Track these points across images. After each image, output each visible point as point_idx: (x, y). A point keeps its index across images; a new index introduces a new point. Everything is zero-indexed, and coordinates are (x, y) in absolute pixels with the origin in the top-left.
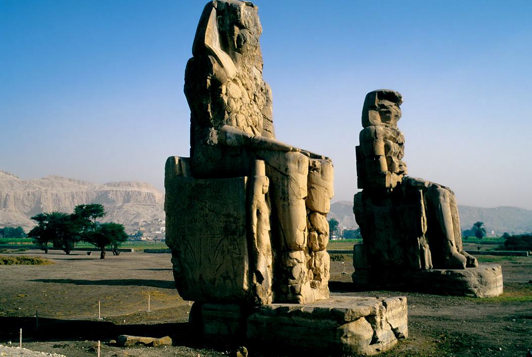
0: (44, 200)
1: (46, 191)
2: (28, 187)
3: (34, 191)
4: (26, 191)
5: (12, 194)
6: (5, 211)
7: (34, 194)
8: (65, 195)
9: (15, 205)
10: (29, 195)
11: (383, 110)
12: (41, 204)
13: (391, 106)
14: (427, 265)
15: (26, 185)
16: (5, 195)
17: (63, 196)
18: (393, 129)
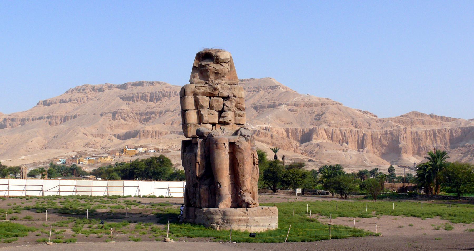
0: (402, 138)
1: (405, 130)
2: (386, 126)
3: (392, 130)
4: (383, 130)
5: (369, 134)
6: (362, 151)
7: (391, 133)
8: (426, 133)
9: (373, 145)
10: (386, 134)
11: (202, 69)
12: (400, 143)
13: (208, 65)
14: (203, 204)
15: (384, 123)
16: (362, 135)
17: (424, 134)
18: (210, 85)
